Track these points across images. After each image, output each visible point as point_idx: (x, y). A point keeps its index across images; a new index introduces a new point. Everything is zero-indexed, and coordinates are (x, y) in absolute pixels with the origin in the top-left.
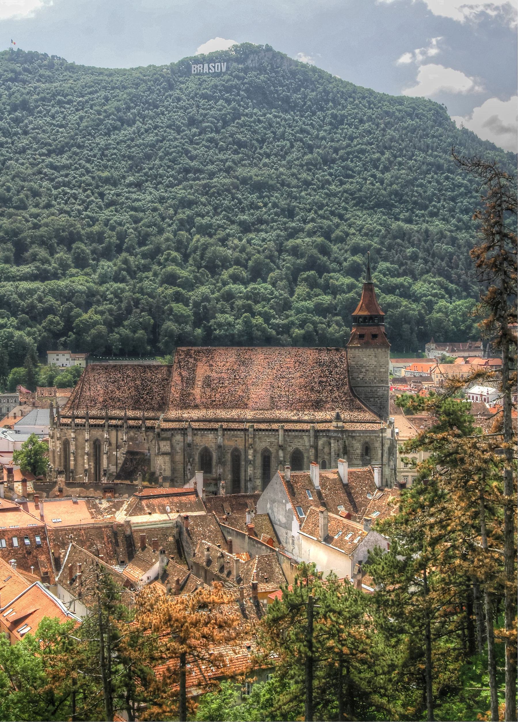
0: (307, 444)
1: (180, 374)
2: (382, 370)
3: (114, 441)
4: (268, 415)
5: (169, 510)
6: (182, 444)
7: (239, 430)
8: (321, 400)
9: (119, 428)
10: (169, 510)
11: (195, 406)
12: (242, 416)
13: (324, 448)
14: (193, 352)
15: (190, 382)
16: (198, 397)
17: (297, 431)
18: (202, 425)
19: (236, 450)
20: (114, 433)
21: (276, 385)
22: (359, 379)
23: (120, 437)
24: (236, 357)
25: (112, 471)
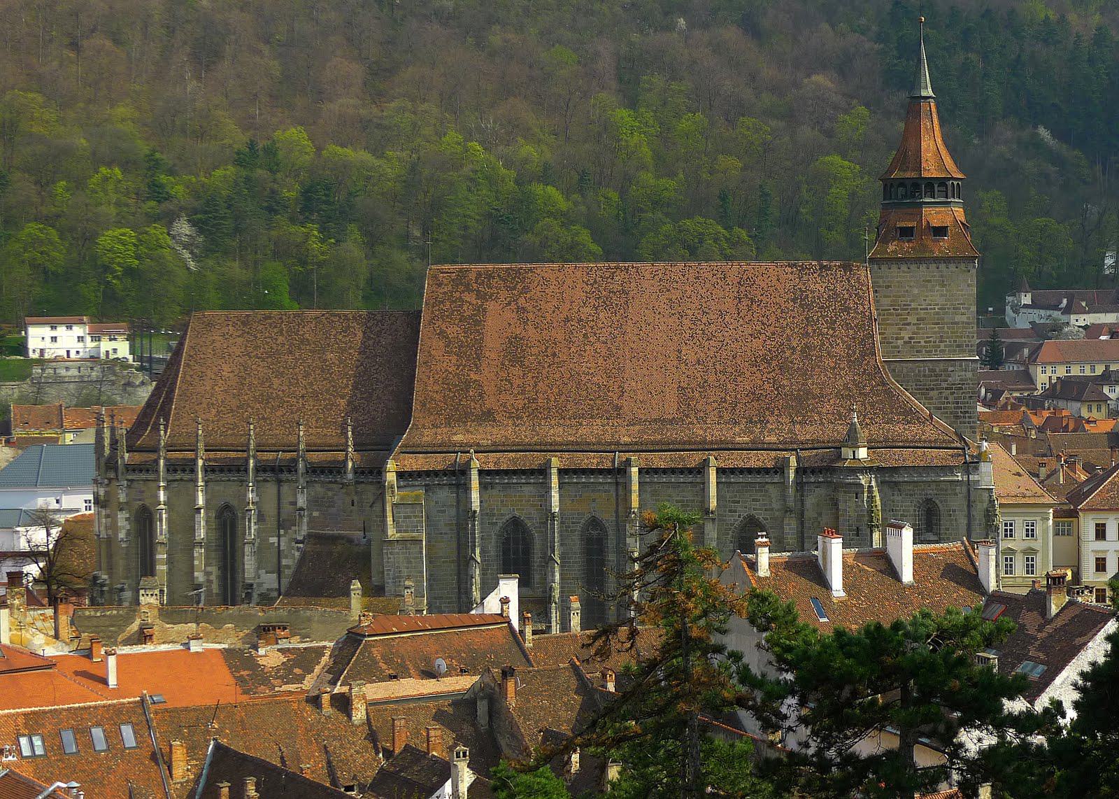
0: (776, 505)
1: (442, 335)
2: (958, 318)
3: (270, 509)
4: (672, 434)
5: (444, 668)
6: (453, 512)
7: (601, 472)
8: (808, 393)
9: (285, 476)
10: (444, 668)
11: (484, 413)
12: (608, 438)
13: (820, 514)
14: (472, 276)
15: (472, 352)
16: (489, 389)
17: (750, 471)
18: (505, 461)
19: (595, 523)
20: (271, 489)
21: (692, 358)
22: (900, 342)
23: (286, 499)
24: (588, 289)
25: (266, 586)
